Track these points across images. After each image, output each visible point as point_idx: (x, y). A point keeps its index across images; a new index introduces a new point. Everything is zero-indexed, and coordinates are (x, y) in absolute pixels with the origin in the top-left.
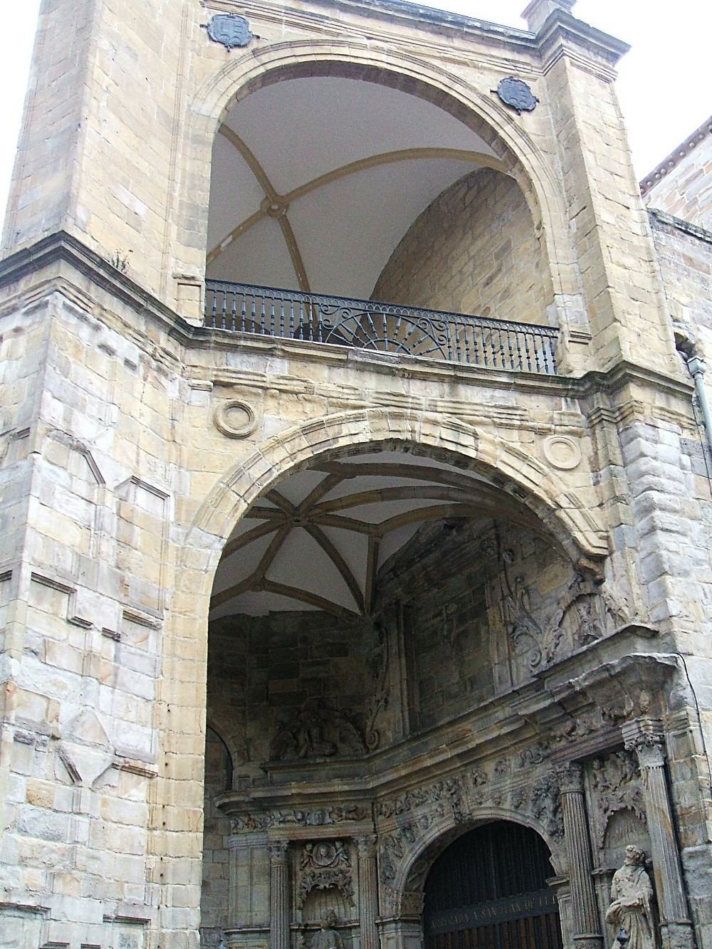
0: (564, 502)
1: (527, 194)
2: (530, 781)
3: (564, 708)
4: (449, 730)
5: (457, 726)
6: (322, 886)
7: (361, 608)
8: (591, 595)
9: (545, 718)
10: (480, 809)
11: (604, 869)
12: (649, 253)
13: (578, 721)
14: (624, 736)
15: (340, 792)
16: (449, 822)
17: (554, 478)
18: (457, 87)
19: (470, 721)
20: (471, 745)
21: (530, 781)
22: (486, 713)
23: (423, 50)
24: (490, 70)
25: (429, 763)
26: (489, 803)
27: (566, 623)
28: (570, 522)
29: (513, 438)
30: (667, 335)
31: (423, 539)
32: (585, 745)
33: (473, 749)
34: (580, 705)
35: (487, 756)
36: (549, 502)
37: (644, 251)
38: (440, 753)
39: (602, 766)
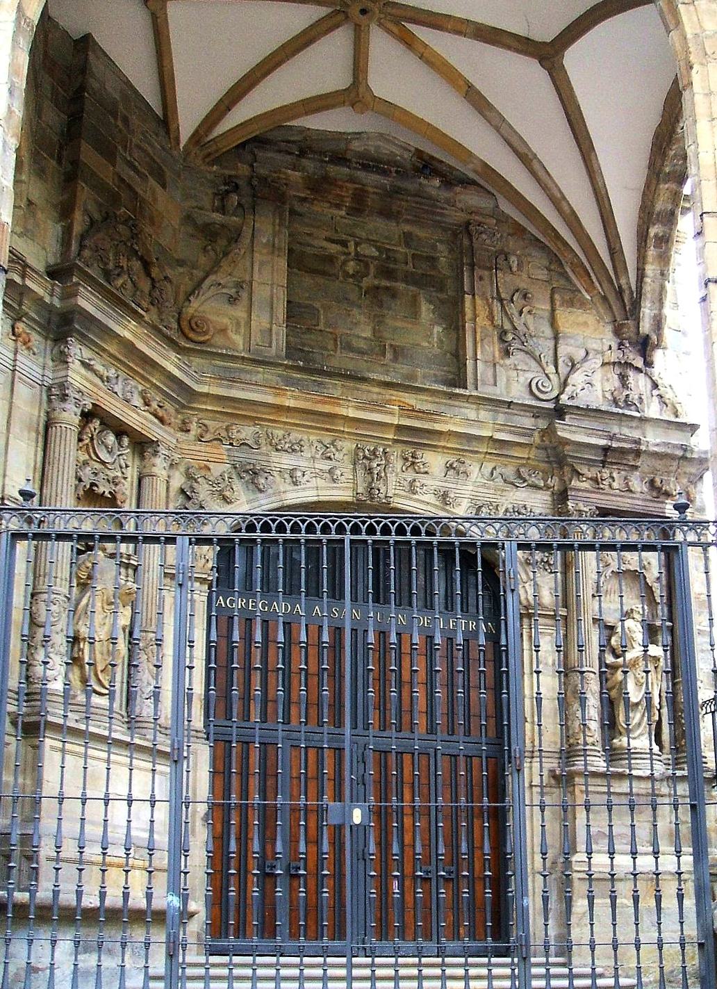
2: (503, 500)
3: (605, 455)
4: (376, 390)
5: (392, 392)
6: (101, 490)
7: (196, 137)
9: (577, 452)
10: (411, 499)
14: (666, 511)
15: (163, 370)
16: (341, 493)
19: (419, 397)
20: (437, 427)
21: (503, 500)
22: (449, 402)
25: (352, 413)
26: (430, 498)
31: (356, 146)
32: (619, 499)
33: (441, 433)
34: (625, 462)
35: (435, 446)
38: (386, 413)
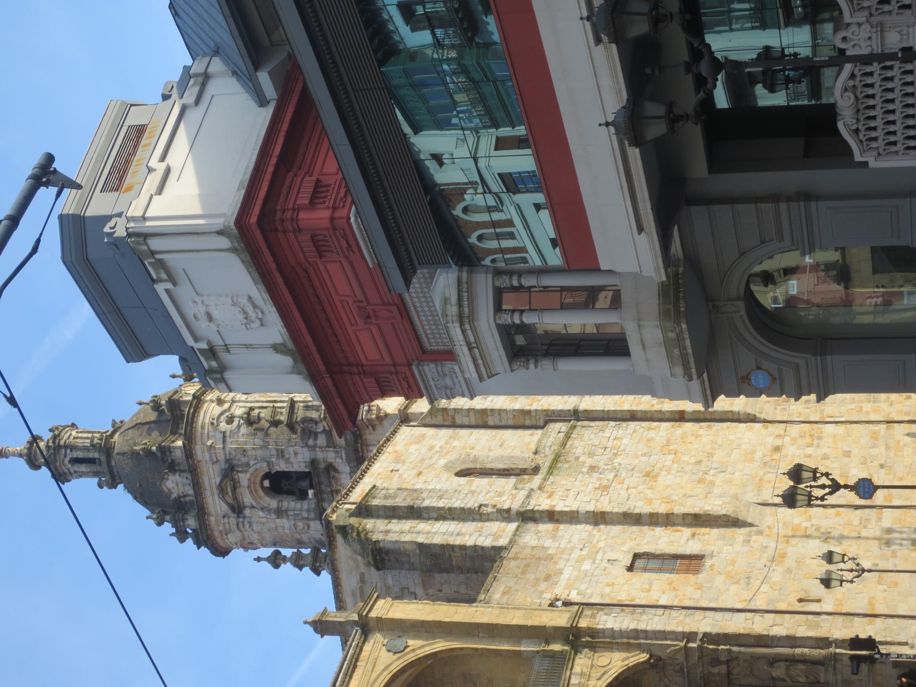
0: (626, 663)
1: (455, 654)
8: (664, 664)
11: (771, 681)
12: (504, 608)
13: (714, 679)
17: (615, 664)
18: (392, 668)
23: (367, 678)
24: (379, 653)
27: (670, 678)
28: (635, 662)
29: (595, 674)
30: (550, 610)
36: (625, 668)
37: (502, 610)
39: (732, 674)
